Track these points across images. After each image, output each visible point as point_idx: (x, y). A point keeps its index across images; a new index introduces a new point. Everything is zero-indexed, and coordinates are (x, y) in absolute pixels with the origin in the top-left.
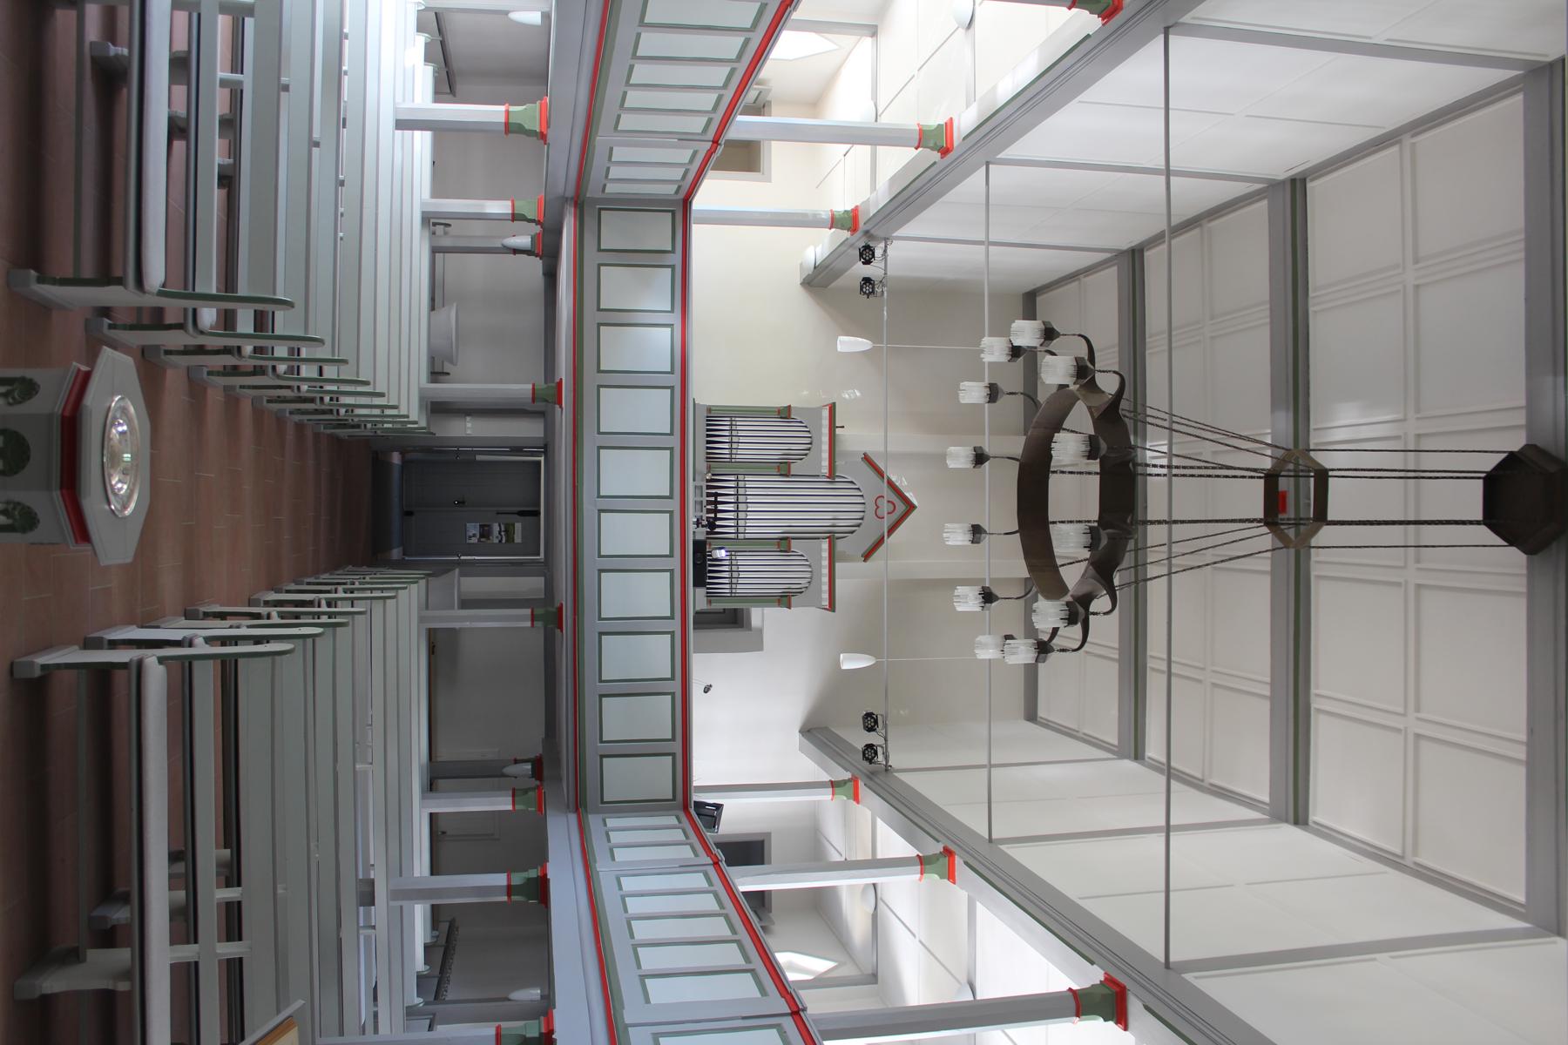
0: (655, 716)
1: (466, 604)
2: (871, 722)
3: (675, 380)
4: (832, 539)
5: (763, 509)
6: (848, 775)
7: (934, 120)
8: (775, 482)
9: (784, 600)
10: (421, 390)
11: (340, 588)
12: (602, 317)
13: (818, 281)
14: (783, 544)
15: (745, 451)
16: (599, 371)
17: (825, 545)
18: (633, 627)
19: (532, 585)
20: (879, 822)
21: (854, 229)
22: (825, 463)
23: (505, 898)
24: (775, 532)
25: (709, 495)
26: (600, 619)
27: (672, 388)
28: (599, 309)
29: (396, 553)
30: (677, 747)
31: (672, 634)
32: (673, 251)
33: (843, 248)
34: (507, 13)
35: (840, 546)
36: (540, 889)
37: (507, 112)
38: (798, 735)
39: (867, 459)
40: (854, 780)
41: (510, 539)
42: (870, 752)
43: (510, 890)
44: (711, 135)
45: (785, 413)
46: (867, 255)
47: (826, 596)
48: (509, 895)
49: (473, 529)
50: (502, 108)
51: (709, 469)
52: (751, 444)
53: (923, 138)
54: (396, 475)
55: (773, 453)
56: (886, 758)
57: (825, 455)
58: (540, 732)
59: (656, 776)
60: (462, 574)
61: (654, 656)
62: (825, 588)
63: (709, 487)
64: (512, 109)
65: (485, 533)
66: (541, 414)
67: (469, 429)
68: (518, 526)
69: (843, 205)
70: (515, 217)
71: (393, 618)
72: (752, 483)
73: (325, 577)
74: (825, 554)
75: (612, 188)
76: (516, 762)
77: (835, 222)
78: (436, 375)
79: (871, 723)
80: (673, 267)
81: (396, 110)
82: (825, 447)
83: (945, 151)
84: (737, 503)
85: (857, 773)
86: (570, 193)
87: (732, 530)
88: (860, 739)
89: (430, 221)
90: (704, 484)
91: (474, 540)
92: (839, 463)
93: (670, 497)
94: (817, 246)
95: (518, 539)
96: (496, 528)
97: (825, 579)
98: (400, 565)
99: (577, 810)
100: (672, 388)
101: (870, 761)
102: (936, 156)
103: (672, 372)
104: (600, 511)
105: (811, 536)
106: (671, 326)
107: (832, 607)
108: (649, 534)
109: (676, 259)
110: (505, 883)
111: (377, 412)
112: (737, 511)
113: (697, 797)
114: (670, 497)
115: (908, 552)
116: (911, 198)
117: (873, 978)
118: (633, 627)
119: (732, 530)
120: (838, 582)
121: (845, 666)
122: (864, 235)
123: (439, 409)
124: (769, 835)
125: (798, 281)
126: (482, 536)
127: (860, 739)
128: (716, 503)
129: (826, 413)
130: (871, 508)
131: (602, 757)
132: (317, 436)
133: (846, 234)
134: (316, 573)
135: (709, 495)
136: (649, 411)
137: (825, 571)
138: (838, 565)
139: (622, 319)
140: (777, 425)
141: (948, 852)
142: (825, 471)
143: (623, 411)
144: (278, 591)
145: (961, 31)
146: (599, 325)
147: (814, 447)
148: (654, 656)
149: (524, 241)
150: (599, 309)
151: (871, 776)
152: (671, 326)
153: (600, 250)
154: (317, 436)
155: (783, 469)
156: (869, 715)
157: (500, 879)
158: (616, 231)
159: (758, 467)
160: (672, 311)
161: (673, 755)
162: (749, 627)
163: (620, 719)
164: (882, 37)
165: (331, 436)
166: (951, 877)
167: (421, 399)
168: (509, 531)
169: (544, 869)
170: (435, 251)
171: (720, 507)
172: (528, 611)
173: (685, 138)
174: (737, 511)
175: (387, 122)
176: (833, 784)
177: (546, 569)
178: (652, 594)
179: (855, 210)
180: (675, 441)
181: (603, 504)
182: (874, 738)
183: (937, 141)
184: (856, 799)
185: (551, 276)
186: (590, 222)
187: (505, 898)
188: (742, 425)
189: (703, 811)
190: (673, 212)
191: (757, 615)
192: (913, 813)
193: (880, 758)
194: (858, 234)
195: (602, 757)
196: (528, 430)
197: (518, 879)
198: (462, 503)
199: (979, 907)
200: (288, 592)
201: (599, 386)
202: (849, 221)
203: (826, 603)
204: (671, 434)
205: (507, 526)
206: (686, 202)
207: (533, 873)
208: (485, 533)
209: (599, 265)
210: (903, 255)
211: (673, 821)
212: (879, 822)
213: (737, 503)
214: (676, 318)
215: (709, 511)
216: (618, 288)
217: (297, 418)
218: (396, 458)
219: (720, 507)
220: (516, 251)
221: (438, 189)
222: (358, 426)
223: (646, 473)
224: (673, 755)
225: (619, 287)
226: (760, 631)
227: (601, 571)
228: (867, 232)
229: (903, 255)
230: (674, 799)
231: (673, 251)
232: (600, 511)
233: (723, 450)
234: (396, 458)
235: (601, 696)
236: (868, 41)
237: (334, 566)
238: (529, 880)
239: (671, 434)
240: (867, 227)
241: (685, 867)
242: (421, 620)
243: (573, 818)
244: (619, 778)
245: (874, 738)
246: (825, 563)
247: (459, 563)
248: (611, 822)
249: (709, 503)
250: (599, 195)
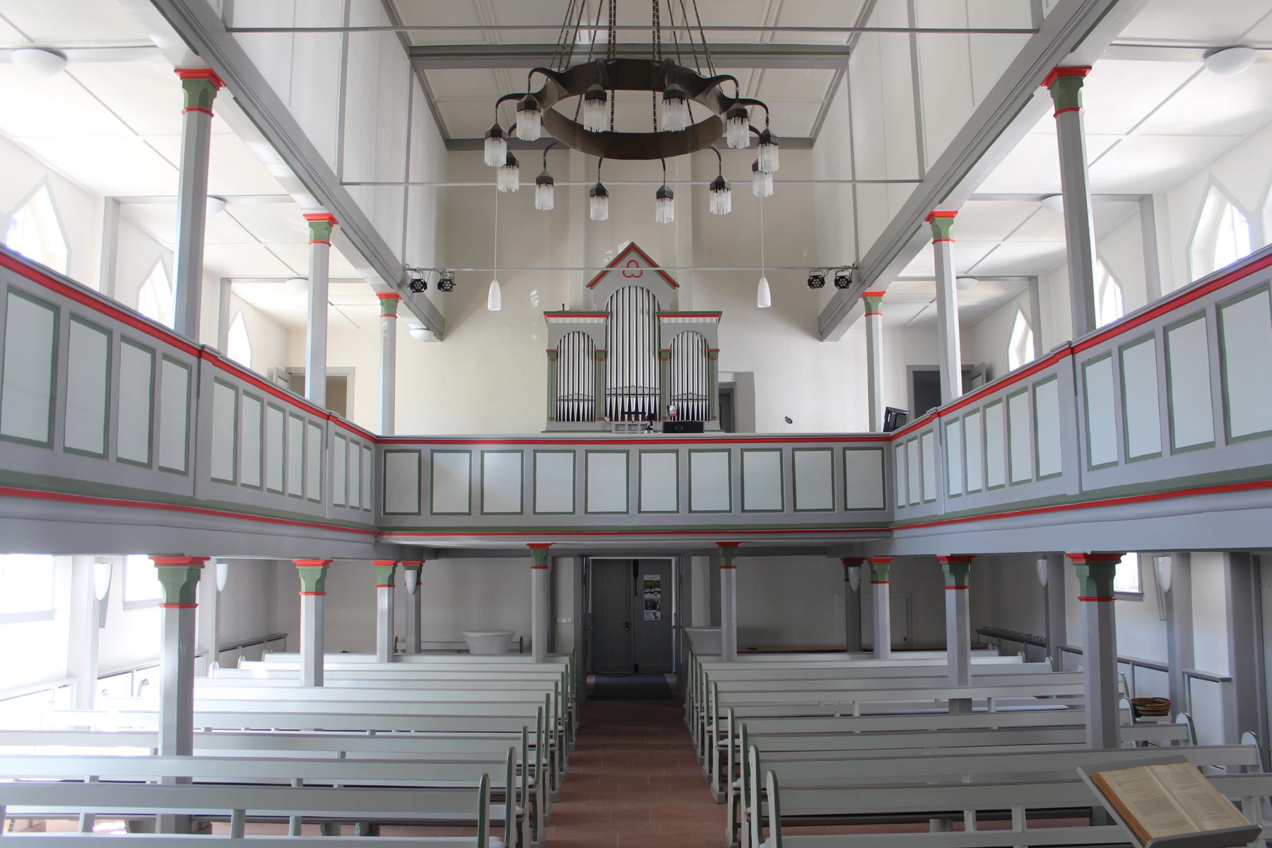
0: (813, 465)
1: (715, 620)
2: (816, 282)
3: (528, 449)
4: (659, 314)
5: (635, 373)
6: (861, 302)
7: (305, 229)
9: (711, 355)
10: (538, 662)
11: (707, 728)
12: (476, 511)
13: (439, 326)
14: (664, 356)
15: (585, 387)
16: (521, 513)
17: (665, 320)
18: (737, 483)
19: (698, 567)
20: (901, 274)
21: (396, 297)
22: (595, 320)
23: (967, 591)
25: (623, 419)
26: (730, 511)
27: (535, 452)
28: (469, 514)
29: (671, 679)
30: (838, 446)
31: (743, 450)
32: (419, 451)
33: (412, 306)
34: (218, 593)
35: (665, 307)
36: (960, 562)
37: (306, 593)
38: (825, 343)
39: (592, 285)
40: (865, 296)
41: (657, 584)
42: (841, 283)
43: (960, 587)
44: (322, 421)
45: (553, 355)
46: (418, 286)
47: (708, 320)
48: (964, 588)
49: (649, 615)
50: (303, 597)
51: (601, 419)
52: (580, 383)
53: (321, 240)
54: (604, 680)
55: (587, 365)
56: (847, 268)
57: (589, 320)
58: (822, 559)
59: (863, 464)
60: (690, 625)
61: (761, 465)
62: (701, 320)
63: (617, 419)
64: (303, 589)
65: (652, 605)
66: (555, 559)
67: (568, 621)
68: (646, 578)
69: (376, 307)
70: (391, 584)
71: (730, 684)
72: (613, 382)
73: (696, 740)
74: (673, 320)
75: (367, 504)
76: (847, 580)
77: (390, 313)
78: (523, 648)
79: (817, 282)
80: (433, 451)
81: (307, 686)
82: (582, 320)
83: (332, 221)
84: (629, 395)
85: (860, 293)
86: (371, 538)
87: (653, 399)
88: (830, 289)
89: (395, 654)
90: (614, 423)
91: (659, 614)
92: (595, 308)
93: (627, 452)
94: (411, 328)
95: (657, 578)
96: (648, 596)
97: (694, 320)
98: (682, 674)
99: (891, 530)
100: (535, 452)
101: (849, 282)
102: (336, 228)
103: (522, 452)
104: (640, 511)
105: (658, 332)
106: (482, 453)
107: (717, 314)
108: (659, 470)
109: (426, 449)
110: (954, 591)
111: (560, 698)
112: (636, 395)
113: (880, 428)
114: (627, 452)
115: (670, 250)
116: (372, 250)
117: (1032, 280)
118: (737, 483)
119: (653, 399)
120: (695, 309)
121: (768, 303)
122: (401, 289)
123: (552, 647)
125: (439, 343)
126: (655, 608)
127: (830, 289)
128: (630, 413)
129: (553, 320)
130: (634, 281)
131: (846, 509)
132: (578, 748)
133: (401, 304)
134: (692, 747)
135: (623, 419)
136: (555, 470)
137: (687, 320)
138: (681, 309)
139: (477, 494)
140: (563, 361)
141: (931, 217)
142: (602, 320)
143: (555, 495)
144: (710, 779)
145: (228, 207)
146: (482, 513)
147: (582, 330)
148: (761, 465)
149: (410, 576)
150: (469, 514)
151: (862, 282)
152: (482, 453)
153: (419, 513)
154: (578, 748)
155: (600, 356)
156: (810, 283)
157: (951, 595)
158: (403, 500)
159: (599, 377)
160: (470, 452)
161: (845, 449)
162: (734, 384)
163: (815, 495)
164: (233, 273)
165: (578, 736)
166: (951, 215)
167: (545, 661)
168: (651, 586)
169: (942, 558)
170: (419, 651)
171: (633, 409)
172: (723, 571)
173: (326, 444)
174: (636, 395)
175: (317, 693)
176: (869, 313)
177: (684, 555)
178: (710, 469)
179: (381, 296)
180: (581, 449)
181: (633, 509)
182: (830, 279)
183: (323, 228)
184: (881, 294)
185: (438, 553)
186: (396, 522)
187: (967, 591)
188: (563, 391)
189: (892, 425)
190: (386, 452)
191: (724, 378)
192: (896, 246)
193: (846, 273)
194: (401, 293)
195: (846, 509)
196: (568, 572)
197: (950, 580)
198: (627, 625)
199: (980, 190)
200: (711, 771)
201: (535, 513)
202: (389, 301)
203: (714, 319)
204: (574, 452)
205: (647, 587)
206: (377, 440)
207: (946, 567)
208: (652, 605)
209: (432, 513)
210: (417, 254)
211: (900, 450)
212: (901, 274)
213: (629, 395)
214: (476, 449)
215: (637, 419)
216: (450, 497)
217: (565, 765)
218: (591, 680)
219: (633, 409)
220: (418, 583)
221: (370, 648)
222: (570, 714)
223: (608, 472)
224: (845, 449)
225: (450, 497)
226: (736, 374)
227: (690, 511)
228: (399, 286)
229: (417, 254)
230: (881, 449)
231: (419, 451)
232: (640, 511)
233: (585, 407)
234: (591, 680)
235: (795, 510)
236: (235, 286)
237: (685, 732)
238: (952, 571)
239: (574, 452)
240: (395, 286)
241: (942, 440)
242: (730, 660)
243: (897, 533)
244: (864, 494)
245: (830, 279)
246: (680, 320)
247: (679, 627)
248: (901, 501)
249: (630, 419)
250: (373, 514)
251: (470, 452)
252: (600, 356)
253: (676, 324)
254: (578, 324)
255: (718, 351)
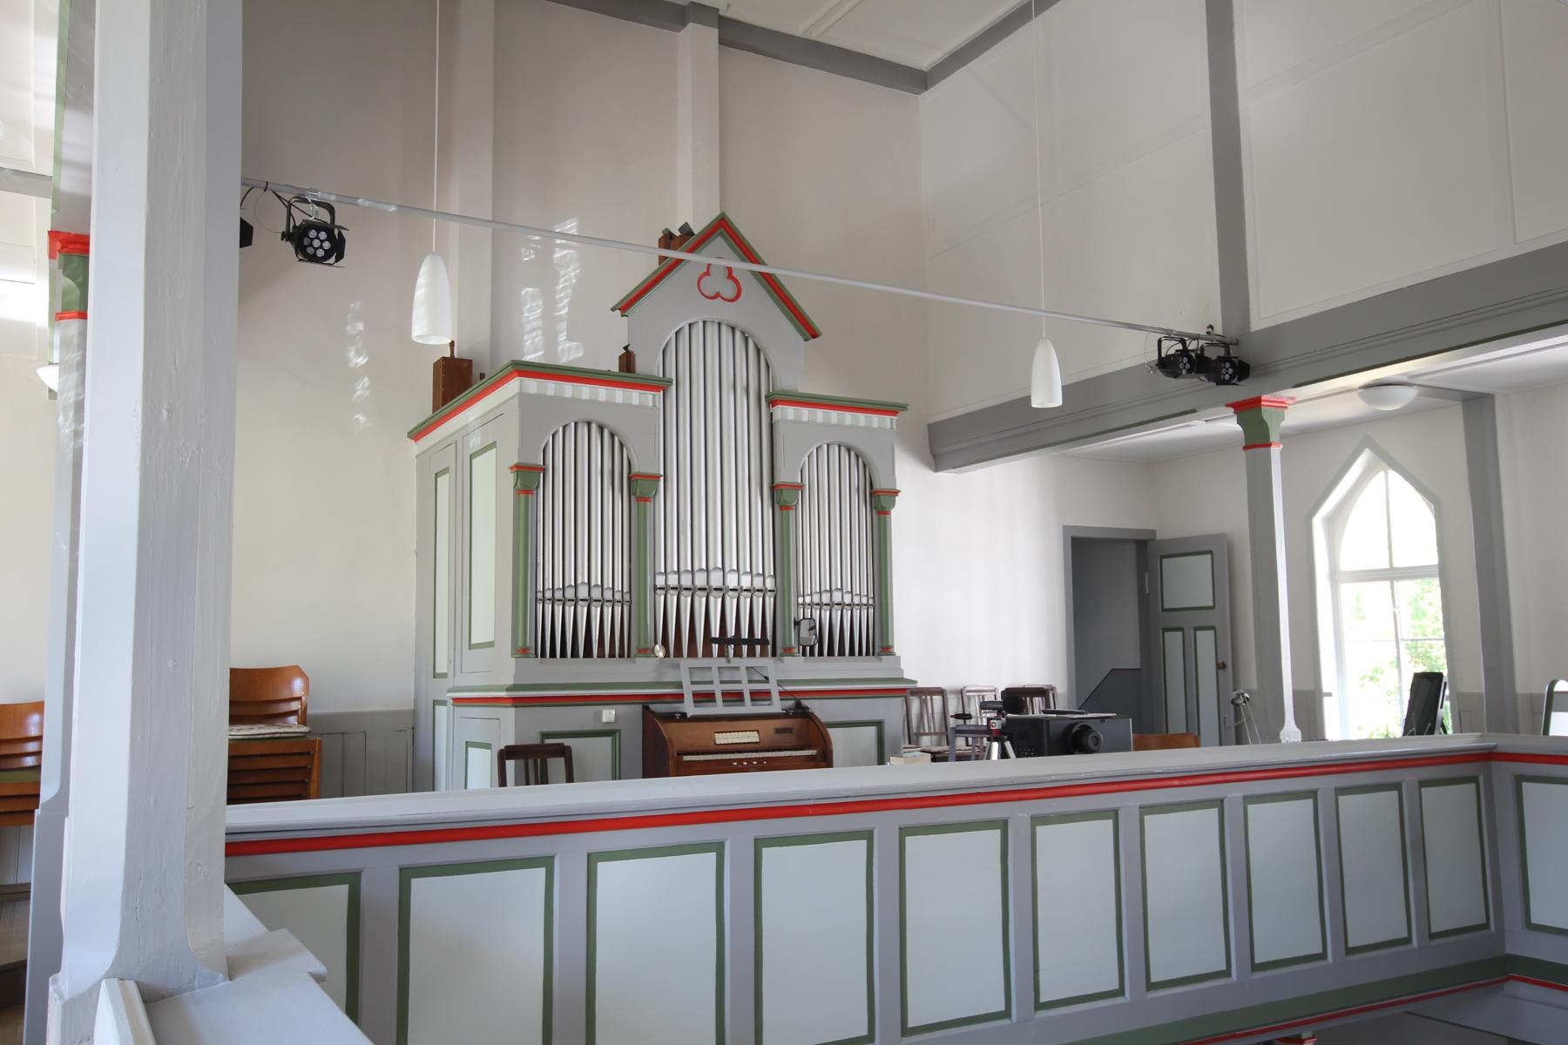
8: (665, 509)
14: (781, 497)
24: (762, 512)
25: (707, 653)
32: (352, 879)
38: (946, 476)
47: (876, 420)
51: (647, 652)
55: (608, 509)
63: (692, 653)
74: (805, 413)
80: (407, 875)
90: (686, 663)
124: (1066, 528)
135: (707, 653)
147: (597, 416)
155: (639, 489)
160: (547, 862)
180: (885, 823)
188: (553, 576)
214: (570, 851)
215: (738, 654)
219: (731, 632)
231: (352, 879)
233: (606, 618)
251: (547, 862)
252: (639, 489)
253: (812, 423)
254: (593, 403)
255: (896, 493)
